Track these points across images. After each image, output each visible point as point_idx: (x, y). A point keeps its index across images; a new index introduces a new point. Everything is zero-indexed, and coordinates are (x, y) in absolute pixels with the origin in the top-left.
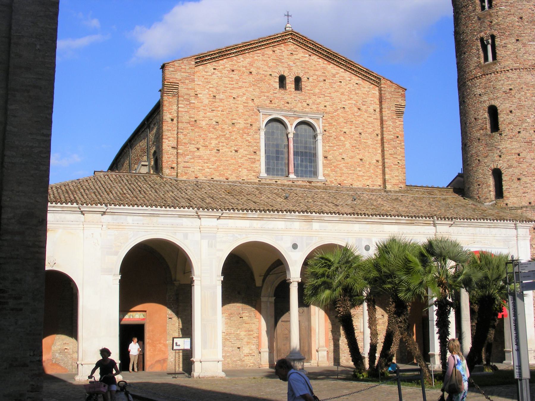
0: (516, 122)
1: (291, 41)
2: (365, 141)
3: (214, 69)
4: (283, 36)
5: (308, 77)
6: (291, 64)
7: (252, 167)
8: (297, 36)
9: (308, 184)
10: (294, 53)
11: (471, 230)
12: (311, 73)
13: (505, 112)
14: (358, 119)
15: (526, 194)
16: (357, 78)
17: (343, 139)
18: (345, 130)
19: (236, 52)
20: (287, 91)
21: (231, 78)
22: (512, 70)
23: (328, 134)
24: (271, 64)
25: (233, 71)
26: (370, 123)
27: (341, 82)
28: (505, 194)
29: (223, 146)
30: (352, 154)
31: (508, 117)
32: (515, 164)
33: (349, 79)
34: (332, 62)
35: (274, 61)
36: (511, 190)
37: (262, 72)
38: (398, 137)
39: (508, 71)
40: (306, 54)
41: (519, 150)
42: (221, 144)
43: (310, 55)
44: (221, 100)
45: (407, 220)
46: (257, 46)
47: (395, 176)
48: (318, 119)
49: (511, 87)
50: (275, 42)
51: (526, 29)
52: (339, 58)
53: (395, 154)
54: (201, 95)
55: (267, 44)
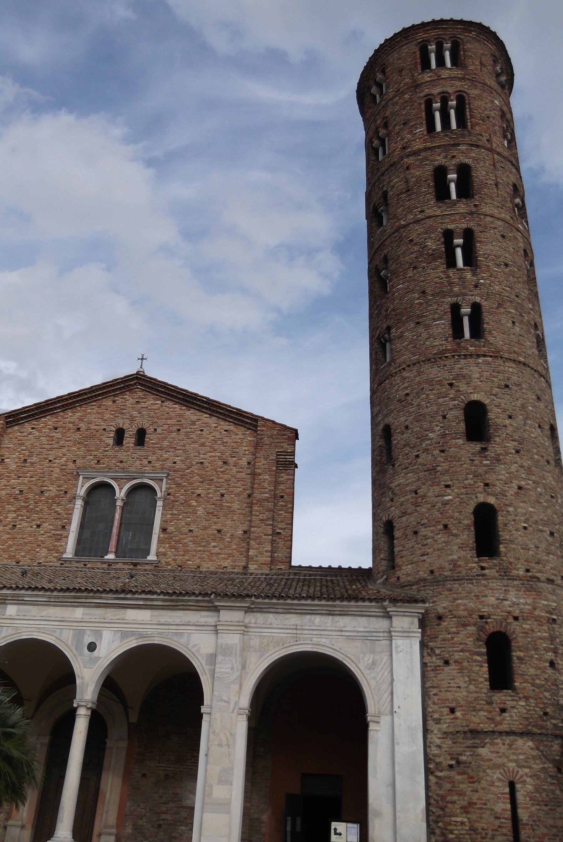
0: (414, 441)
1: (139, 387)
2: (229, 504)
3: (33, 428)
4: (126, 381)
5: (156, 428)
6: (135, 413)
7: (55, 546)
8: (144, 380)
9: (131, 567)
10: (140, 400)
11: (293, 619)
12: (160, 422)
13: (398, 431)
14: (221, 475)
15: (425, 557)
16: (227, 423)
17: (194, 503)
18: (198, 492)
19: (63, 406)
20: (124, 448)
21: (52, 437)
22: (409, 366)
23: (173, 499)
24: (107, 416)
25: (56, 429)
26: (239, 480)
27: (202, 430)
28: (398, 561)
29: (22, 520)
30: (206, 524)
31: (402, 437)
32: (411, 508)
33: (215, 425)
34: (192, 406)
35: (113, 413)
36: (404, 553)
37: (93, 427)
38: (282, 497)
39: (404, 369)
40: (158, 400)
41: (416, 484)
42: (20, 518)
43: (163, 402)
44: (32, 464)
45: (164, 600)
46: (91, 397)
47: (266, 551)
48: (162, 480)
49: (406, 392)
50: (116, 390)
51: (431, 305)
52: (199, 400)
53: (268, 519)
54: (9, 460)
55: (105, 392)
